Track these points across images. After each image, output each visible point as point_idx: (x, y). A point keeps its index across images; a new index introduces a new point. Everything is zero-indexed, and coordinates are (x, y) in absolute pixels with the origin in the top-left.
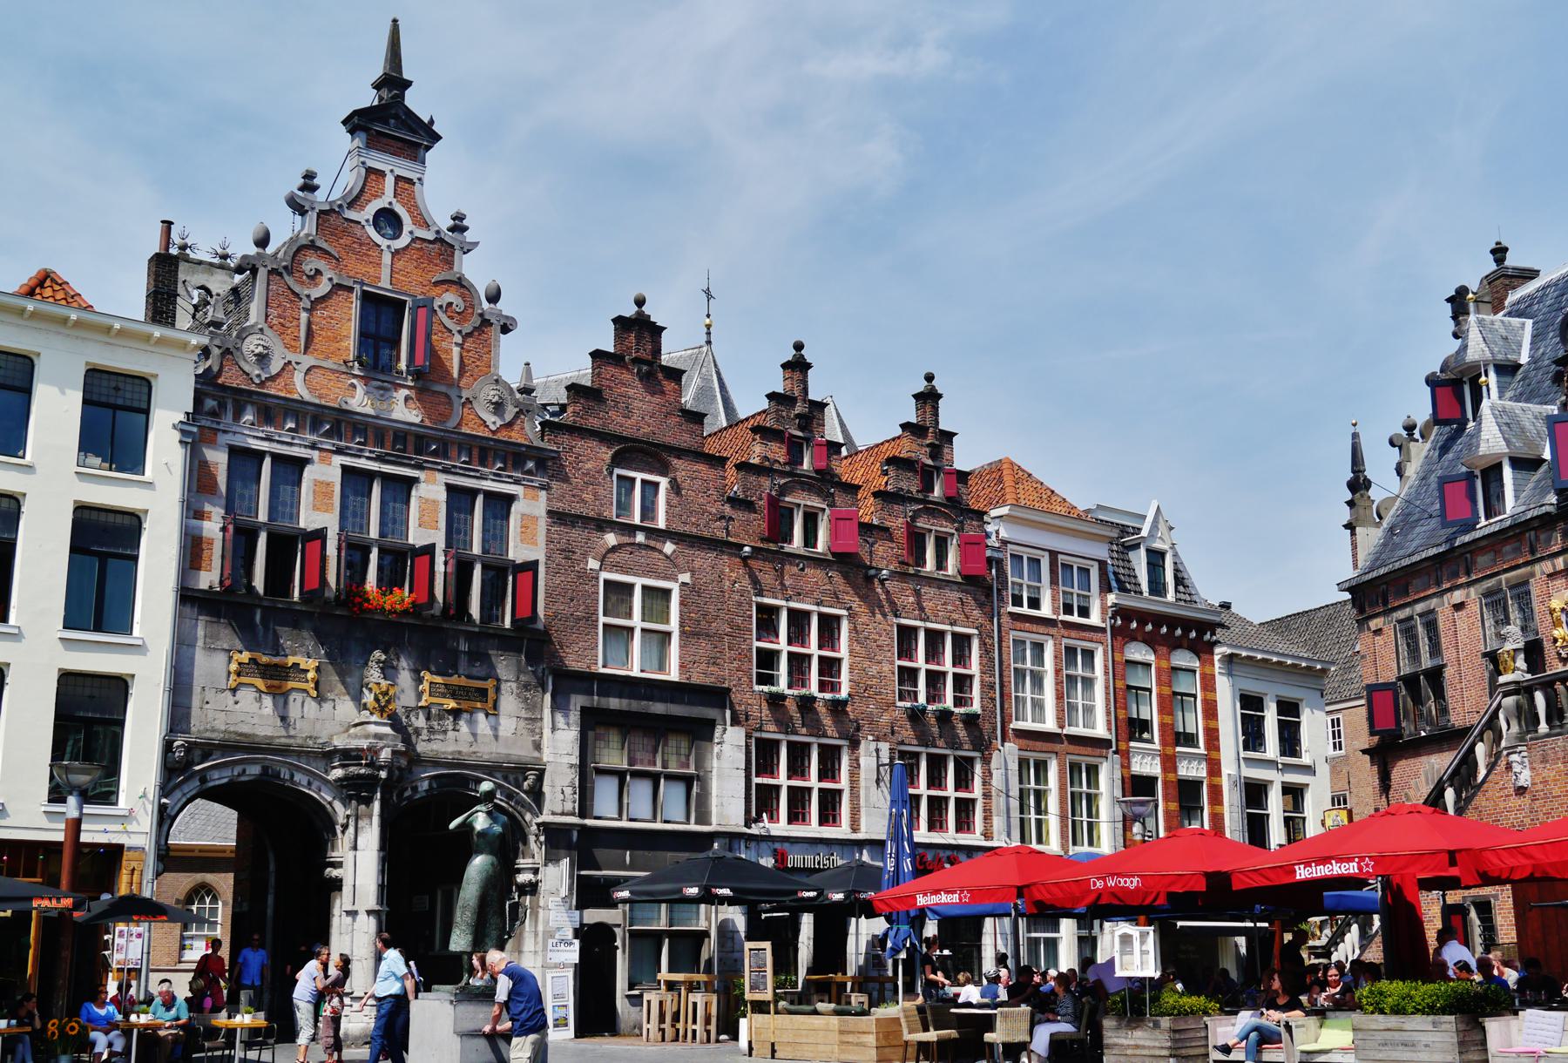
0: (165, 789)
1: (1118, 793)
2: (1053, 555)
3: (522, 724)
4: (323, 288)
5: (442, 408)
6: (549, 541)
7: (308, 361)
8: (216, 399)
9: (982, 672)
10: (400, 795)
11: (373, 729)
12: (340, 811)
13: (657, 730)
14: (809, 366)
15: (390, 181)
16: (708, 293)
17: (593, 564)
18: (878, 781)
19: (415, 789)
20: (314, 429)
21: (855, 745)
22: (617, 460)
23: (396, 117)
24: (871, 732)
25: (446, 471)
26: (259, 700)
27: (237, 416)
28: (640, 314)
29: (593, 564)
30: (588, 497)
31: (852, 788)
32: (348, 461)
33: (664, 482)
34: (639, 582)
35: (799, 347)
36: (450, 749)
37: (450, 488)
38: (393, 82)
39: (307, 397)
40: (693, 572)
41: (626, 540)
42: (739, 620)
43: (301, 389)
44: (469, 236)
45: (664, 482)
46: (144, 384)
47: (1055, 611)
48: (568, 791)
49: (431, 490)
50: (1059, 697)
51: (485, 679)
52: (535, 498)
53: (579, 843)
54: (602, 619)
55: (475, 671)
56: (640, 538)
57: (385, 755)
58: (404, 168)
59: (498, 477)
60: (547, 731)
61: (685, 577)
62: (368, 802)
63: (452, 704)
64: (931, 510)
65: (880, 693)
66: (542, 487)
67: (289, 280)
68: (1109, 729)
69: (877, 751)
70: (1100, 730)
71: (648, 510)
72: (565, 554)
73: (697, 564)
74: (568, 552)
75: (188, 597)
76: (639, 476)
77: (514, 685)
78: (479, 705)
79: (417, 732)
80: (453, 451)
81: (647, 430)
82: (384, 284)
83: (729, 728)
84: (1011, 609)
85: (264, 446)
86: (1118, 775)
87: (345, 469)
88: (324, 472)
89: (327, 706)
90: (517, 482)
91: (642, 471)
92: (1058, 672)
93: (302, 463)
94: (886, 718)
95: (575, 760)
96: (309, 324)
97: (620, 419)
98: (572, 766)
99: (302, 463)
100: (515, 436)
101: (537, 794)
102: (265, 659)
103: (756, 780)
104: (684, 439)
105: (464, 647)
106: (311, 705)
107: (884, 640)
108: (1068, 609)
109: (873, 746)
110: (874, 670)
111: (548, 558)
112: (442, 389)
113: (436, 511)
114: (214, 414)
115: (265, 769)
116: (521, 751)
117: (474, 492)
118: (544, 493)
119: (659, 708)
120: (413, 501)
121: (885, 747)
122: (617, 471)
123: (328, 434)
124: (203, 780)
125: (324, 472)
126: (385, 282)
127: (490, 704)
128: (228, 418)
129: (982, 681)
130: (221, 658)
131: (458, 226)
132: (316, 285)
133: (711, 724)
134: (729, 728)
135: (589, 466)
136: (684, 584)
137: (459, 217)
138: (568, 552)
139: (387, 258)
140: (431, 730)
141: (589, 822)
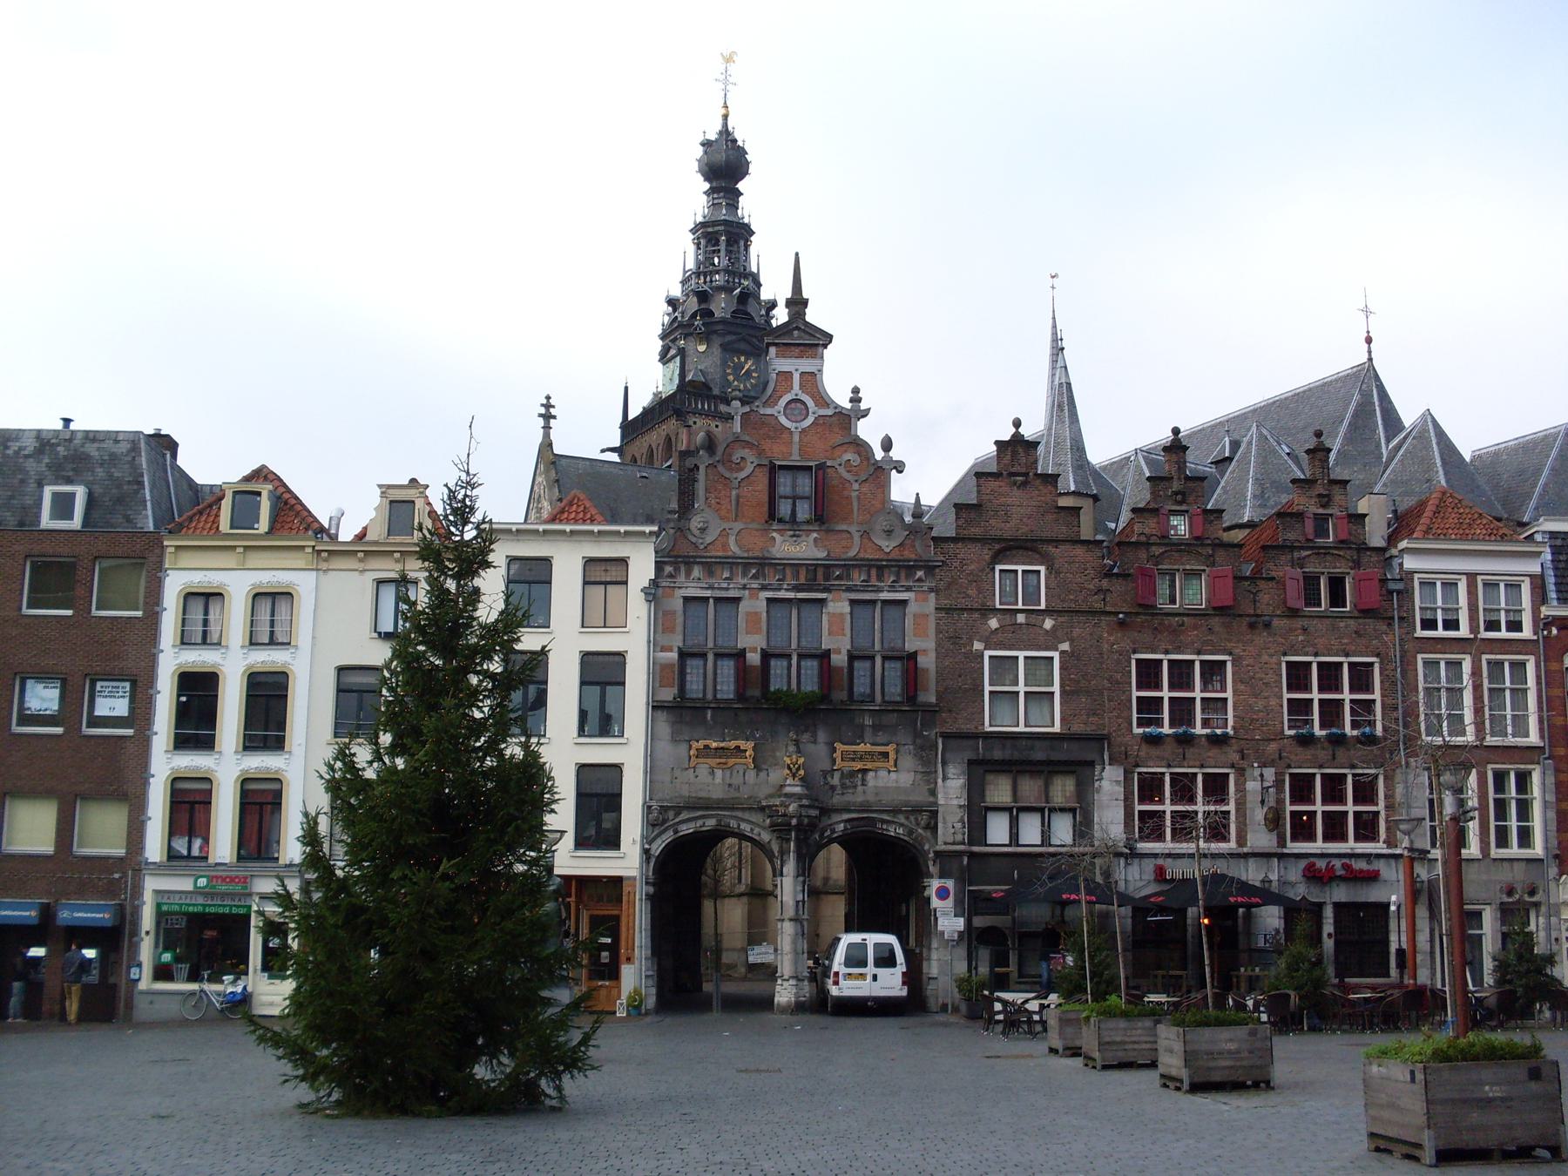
0: (648, 839)
1: (1551, 798)
2: (1472, 577)
4: (749, 469)
5: (844, 543)
6: (938, 631)
7: (738, 526)
10: (822, 835)
11: (788, 790)
12: (775, 848)
13: (1047, 769)
14: (1185, 448)
15: (796, 377)
16: (1367, 311)
17: (977, 646)
18: (1263, 802)
19: (833, 831)
20: (744, 575)
21: (1241, 772)
22: (996, 559)
23: (797, 328)
24: (1257, 759)
25: (849, 589)
27: (688, 574)
29: (977, 646)
31: (1237, 810)
32: (770, 594)
33: (1042, 569)
34: (1021, 655)
36: (860, 799)
37: (853, 602)
39: (739, 553)
40: (1072, 641)
43: (734, 548)
44: (863, 406)
45: (1042, 569)
46: (623, 562)
47: (1474, 628)
49: (839, 606)
50: (1478, 711)
52: (926, 600)
53: (973, 865)
54: (987, 688)
55: (879, 740)
56: (1021, 618)
57: (792, 808)
58: (806, 365)
59: (892, 589)
60: (940, 781)
61: (1065, 646)
62: (788, 840)
63: (859, 765)
64: (1322, 552)
66: (931, 590)
67: (721, 468)
68: (1542, 737)
69: (1262, 775)
70: (1534, 738)
71: (1031, 595)
72: (953, 642)
73: (1075, 634)
74: (955, 639)
75: (656, 707)
76: (1020, 568)
79: (833, 788)
80: (855, 574)
81: (1025, 529)
82: (795, 459)
84: (1420, 633)
85: (708, 593)
86: (1551, 780)
87: (769, 600)
88: (754, 604)
89: (763, 774)
90: (909, 589)
92: (1477, 688)
93: (737, 600)
95: (963, 802)
96: (738, 496)
99: (737, 600)
100: (908, 554)
101: (933, 828)
102: (714, 745)
103: (1138, 807)
104: (1062, 531)
105: (868, 721)
106: (751, 774)
107: (1271, 678)
108: (1493, 625)
109: (1257, 772)
110: (1260, 704)
111: (938, 645)
112: (844, 527)
113: (843, 621)
114: (671, 576)
115: (719, 821)
116: (920, 797)
117: (874, 602)
119: (1039, 755)
120: (825, 618)
121: (1270, 773)
122: (998, 567)
123: (755, 577)
124: (676, 832)
125: (754, 604)
126: (796, 456)
127: (892, 762)
128: (682, 578)
130: (684, 746)
131: (856, 399)
132: (742, 469)
133: (1092, 764)
136: (1062, 652)
137: (856, 390)
138: (955, 639)
139: (796, 438)
140: (843, 786)
141: (976, 849)
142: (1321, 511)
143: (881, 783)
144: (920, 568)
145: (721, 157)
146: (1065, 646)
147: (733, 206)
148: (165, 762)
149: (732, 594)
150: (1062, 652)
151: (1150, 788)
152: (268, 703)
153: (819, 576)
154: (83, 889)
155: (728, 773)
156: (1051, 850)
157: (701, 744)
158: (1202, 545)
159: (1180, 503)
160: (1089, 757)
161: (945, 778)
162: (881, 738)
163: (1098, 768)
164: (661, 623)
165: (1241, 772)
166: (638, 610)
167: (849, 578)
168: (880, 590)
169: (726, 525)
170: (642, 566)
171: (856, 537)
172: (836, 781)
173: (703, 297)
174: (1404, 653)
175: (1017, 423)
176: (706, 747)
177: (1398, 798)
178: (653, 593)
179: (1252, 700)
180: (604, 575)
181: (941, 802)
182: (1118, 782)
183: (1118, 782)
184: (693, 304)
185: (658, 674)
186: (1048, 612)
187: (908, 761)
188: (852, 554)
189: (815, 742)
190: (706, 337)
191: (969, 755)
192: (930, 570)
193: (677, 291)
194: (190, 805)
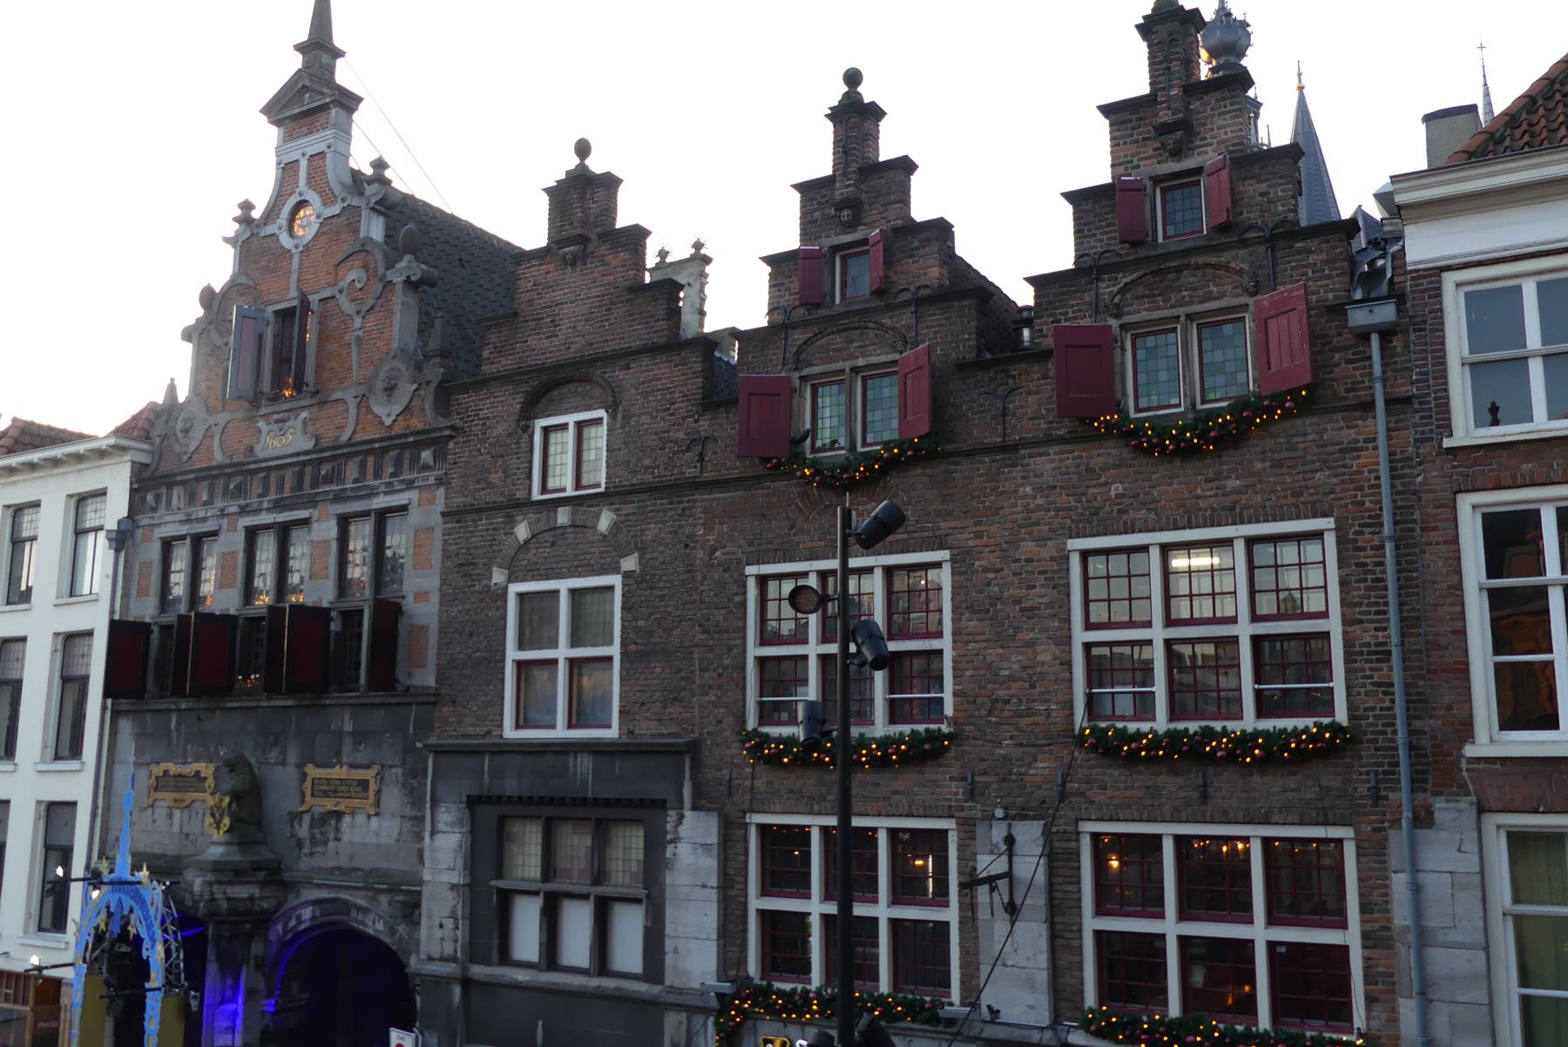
3: (407, 825)
6: (446, 556)
9: (1346, 621)
10: (285, 925)
17: (498, 577)
22: (531, 409)
25: (339, 498)
26: (170, 816)
28: (582, 167)
30: (496, 478)
34: (563, 586)
35: (853, 78)
38: (319, 48)
40: (642, 551)
41: (542, 526)
42: (719, 616)
48: (449, 924)
51: (368, 767)
52: (431, 501)
60: (427, 835)
61: (630, 563)
63: (329, 804)
65: (1030, 713)
66: (440, 482)
69: (1010, 840)
72: (464, 571)
73: (649, 535)
77: (399, 771)
78: (356, 803)
79: (300, 843)
83: (688, 814)
90: (410, 485)
91: (578, 409)
94: (1043, 767)
95: (456, 878)
97: (545, 343)
98: (453, 887)
102: (173, 769)
107: (1040, 595)
109: (998, 832)
110: (1014, 663)
113: (327, 554)
118: (441, 491)
129: (1348, 644)
133: (662, 805)
134: (688, 814)
135: (499, 430)
136: (627, 575)
140: (314, 843)
142: (1173, 167)
143: (358, 838)
144: (425, 444)
146: (630, 563)
149: (210, 526)
150: (627, 575)
151: (784, 859)
155: (186, 813)
156: (609, 983)
157: (158, 770)
158: (891, 308)
159: (852, 225)
160: (660, 791)
161: (433, 833)
162: (362, 756)
163: (672, 815)
165: (968, 829)
167: (341, 481)
168: (372, 494)
169: (211, 420)
171: (352, 404)
172: (303, 831)
174: (1406, 497)
175: (583, 149)
176: (166, 772)
177: (1401, 916)
179: (993, 653)
181: (426, 877)
182: (706, 847)
183: (706, 847)
186: (609, 497)
187: (394, 798)
188: (345, 438)
189: (283, 763)
191: (468, 787)
192: (438, 443)
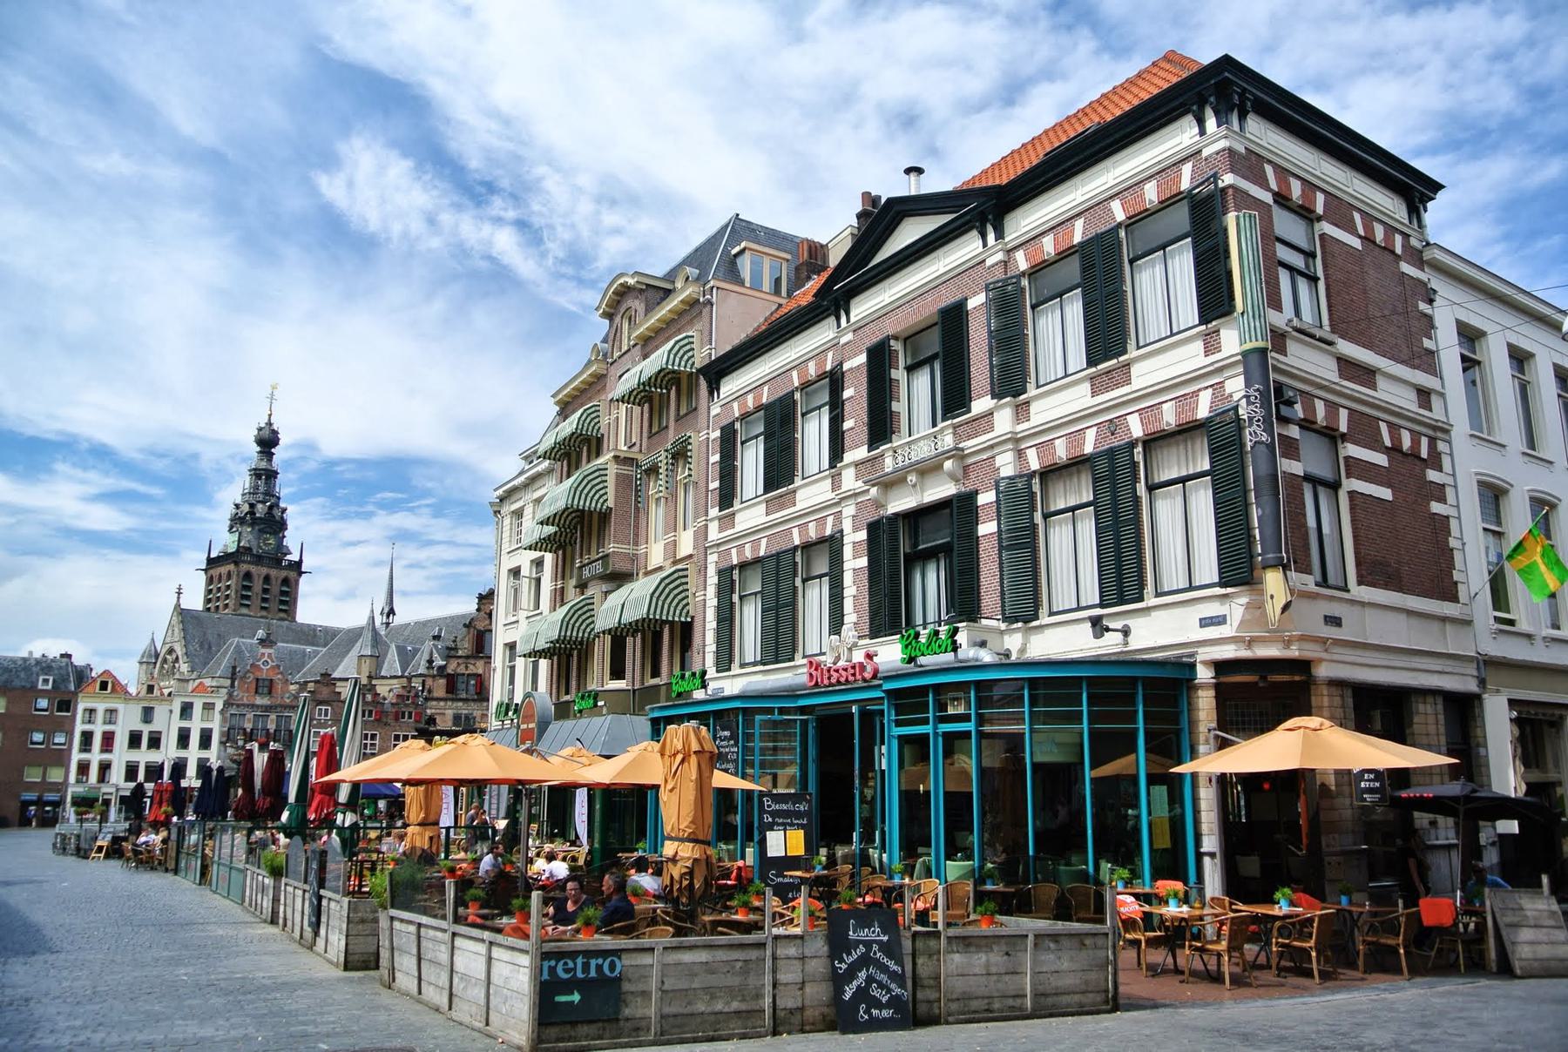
8: (227, 704)
125: (250, 716)
145: (266, 433)
147: (270, 460)
148: (76, 756)
152: (108, 740)
153: (268, 709)
154: (50, 791)
164: (224, 720)
166: (217, 717)
170: (219, 706)
173: (252, 506)
178: (222, 712)
180: (209, 707)
184: (246, 508)
185: (222, 734)
190: (252, 525)
193: (239, 501)
194: (83, 768)
